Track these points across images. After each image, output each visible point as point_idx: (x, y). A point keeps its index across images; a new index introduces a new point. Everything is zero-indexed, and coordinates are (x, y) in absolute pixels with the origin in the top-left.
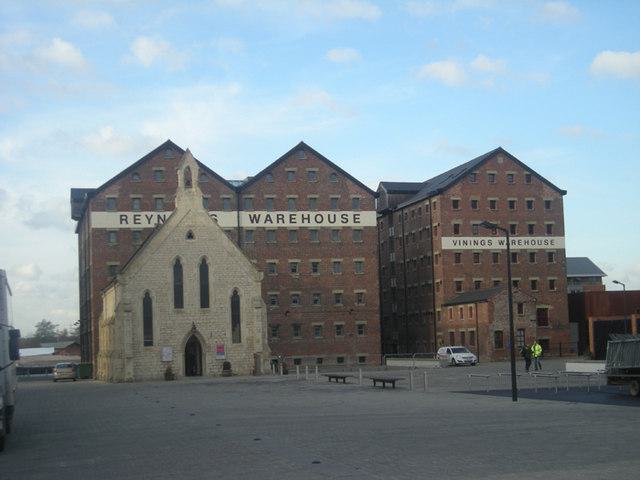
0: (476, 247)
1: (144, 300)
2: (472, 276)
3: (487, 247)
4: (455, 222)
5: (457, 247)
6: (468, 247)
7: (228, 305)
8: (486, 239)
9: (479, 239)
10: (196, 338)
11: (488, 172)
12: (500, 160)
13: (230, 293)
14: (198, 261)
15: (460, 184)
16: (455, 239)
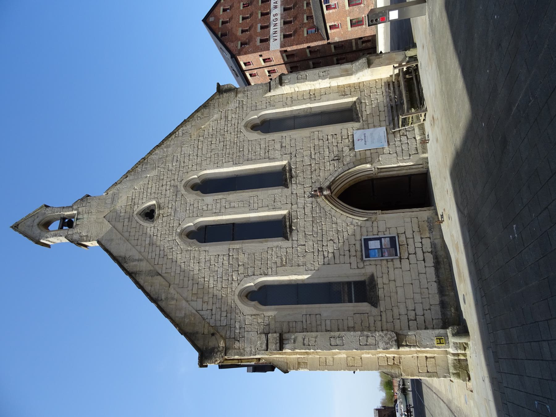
0: (279, 25)
1: (264, 302)
2: (303, 24)
3: (279, 17)
4: (258, 43)
5: (278, 38)
6: (279, 30)
7: (276, 136)
8: (272, 18)
9: (272, 23)
10: (339, 188)
11: (220, 26)
12: (211, 19)
13: (255, 136)
14: (193, 197)
15: (228, 44)
16: (271, 40)
